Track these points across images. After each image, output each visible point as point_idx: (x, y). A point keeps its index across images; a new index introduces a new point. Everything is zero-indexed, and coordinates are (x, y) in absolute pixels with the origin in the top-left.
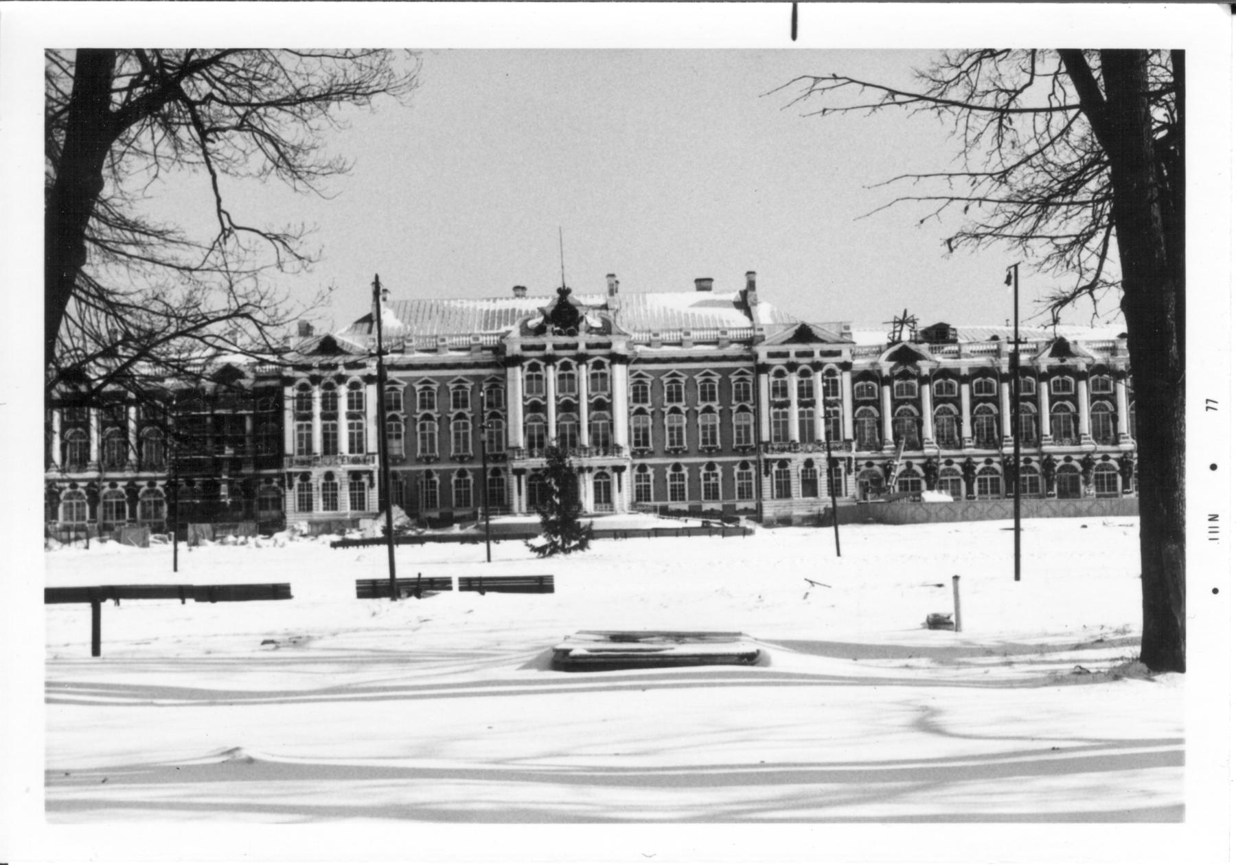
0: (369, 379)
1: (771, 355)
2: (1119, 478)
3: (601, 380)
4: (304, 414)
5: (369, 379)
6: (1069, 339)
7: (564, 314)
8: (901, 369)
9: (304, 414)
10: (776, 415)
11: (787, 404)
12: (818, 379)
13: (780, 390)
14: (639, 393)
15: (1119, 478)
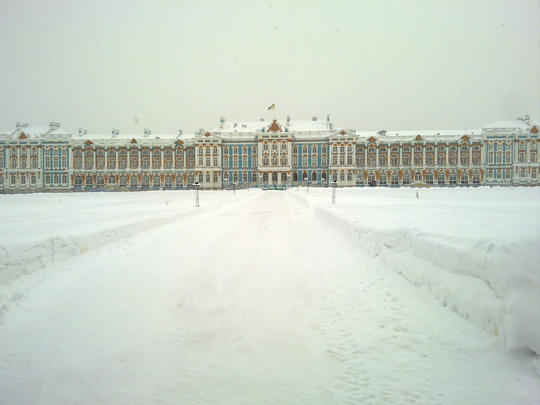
0: (219, 145)
1: (333, 140)
2: (445, 177)
3: (284, 147)
4: (201, 155)
5: (219, 145)
6: (421, 135)
7: (275, 127)
8: (370, 144)
9: (201, 155)
10: (334, 157)
11: (337, 154)
12: (346, 147)
13: (335, 149)
14: (295, 151)
15: (445, 177)
